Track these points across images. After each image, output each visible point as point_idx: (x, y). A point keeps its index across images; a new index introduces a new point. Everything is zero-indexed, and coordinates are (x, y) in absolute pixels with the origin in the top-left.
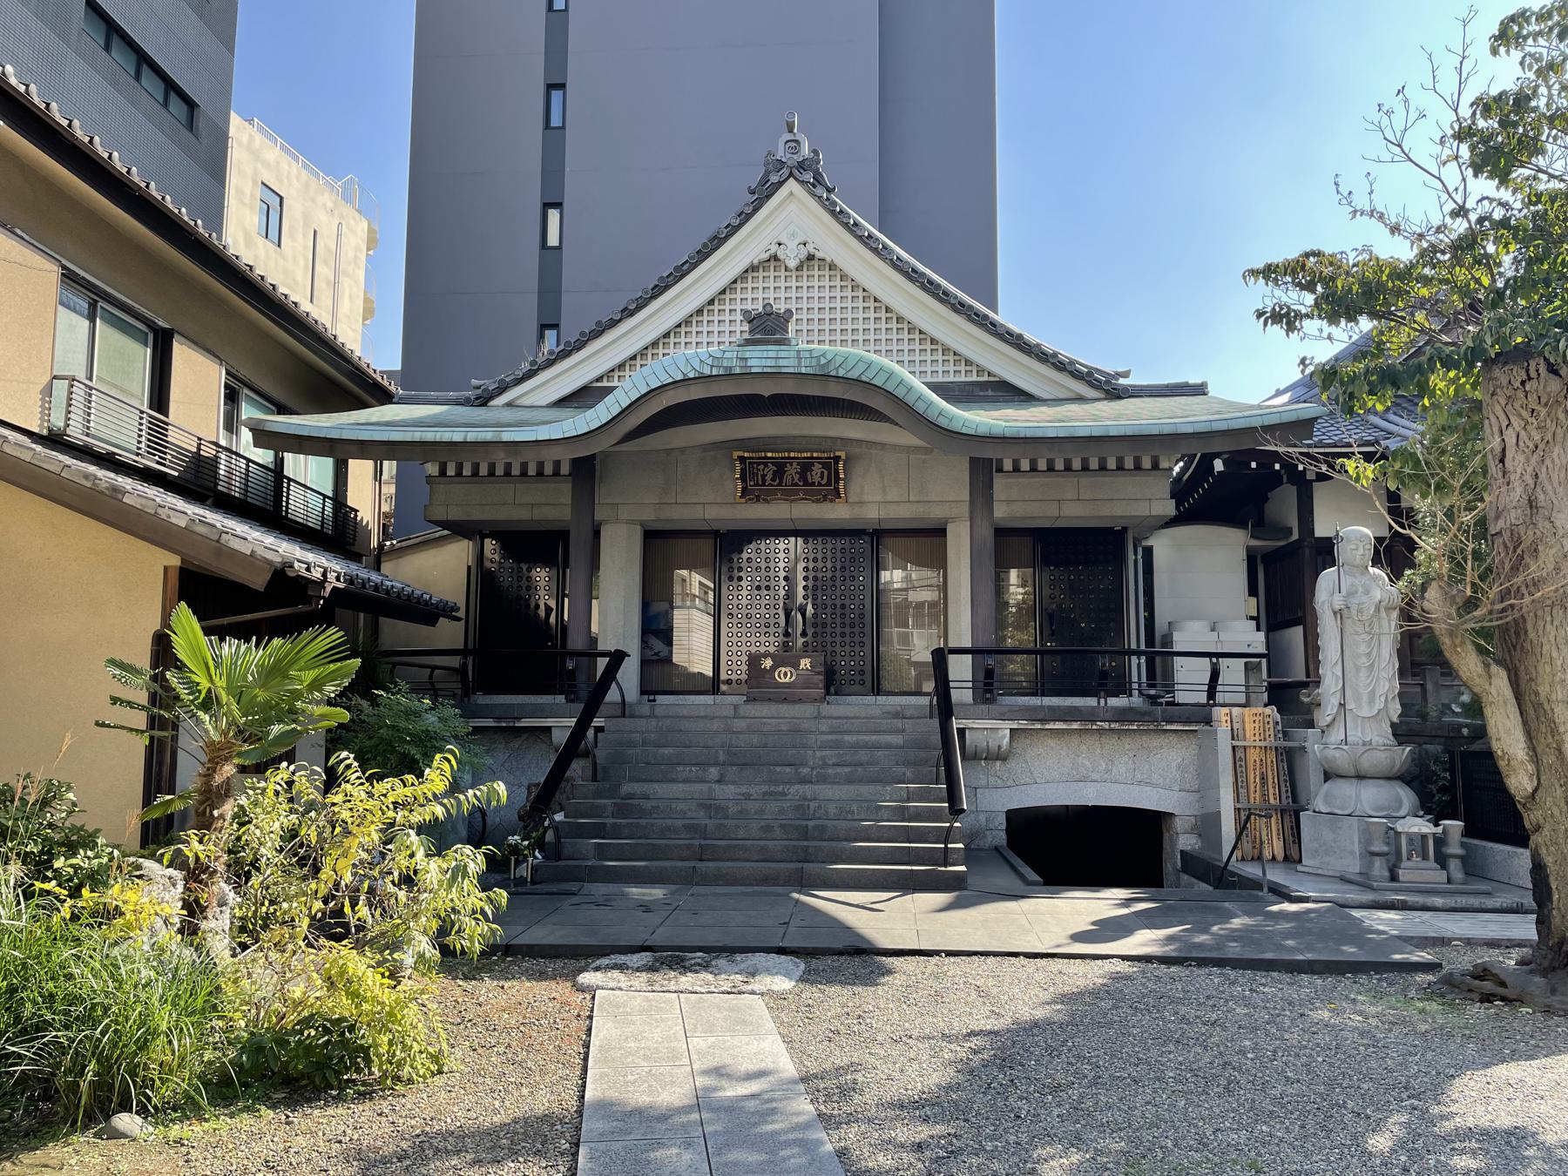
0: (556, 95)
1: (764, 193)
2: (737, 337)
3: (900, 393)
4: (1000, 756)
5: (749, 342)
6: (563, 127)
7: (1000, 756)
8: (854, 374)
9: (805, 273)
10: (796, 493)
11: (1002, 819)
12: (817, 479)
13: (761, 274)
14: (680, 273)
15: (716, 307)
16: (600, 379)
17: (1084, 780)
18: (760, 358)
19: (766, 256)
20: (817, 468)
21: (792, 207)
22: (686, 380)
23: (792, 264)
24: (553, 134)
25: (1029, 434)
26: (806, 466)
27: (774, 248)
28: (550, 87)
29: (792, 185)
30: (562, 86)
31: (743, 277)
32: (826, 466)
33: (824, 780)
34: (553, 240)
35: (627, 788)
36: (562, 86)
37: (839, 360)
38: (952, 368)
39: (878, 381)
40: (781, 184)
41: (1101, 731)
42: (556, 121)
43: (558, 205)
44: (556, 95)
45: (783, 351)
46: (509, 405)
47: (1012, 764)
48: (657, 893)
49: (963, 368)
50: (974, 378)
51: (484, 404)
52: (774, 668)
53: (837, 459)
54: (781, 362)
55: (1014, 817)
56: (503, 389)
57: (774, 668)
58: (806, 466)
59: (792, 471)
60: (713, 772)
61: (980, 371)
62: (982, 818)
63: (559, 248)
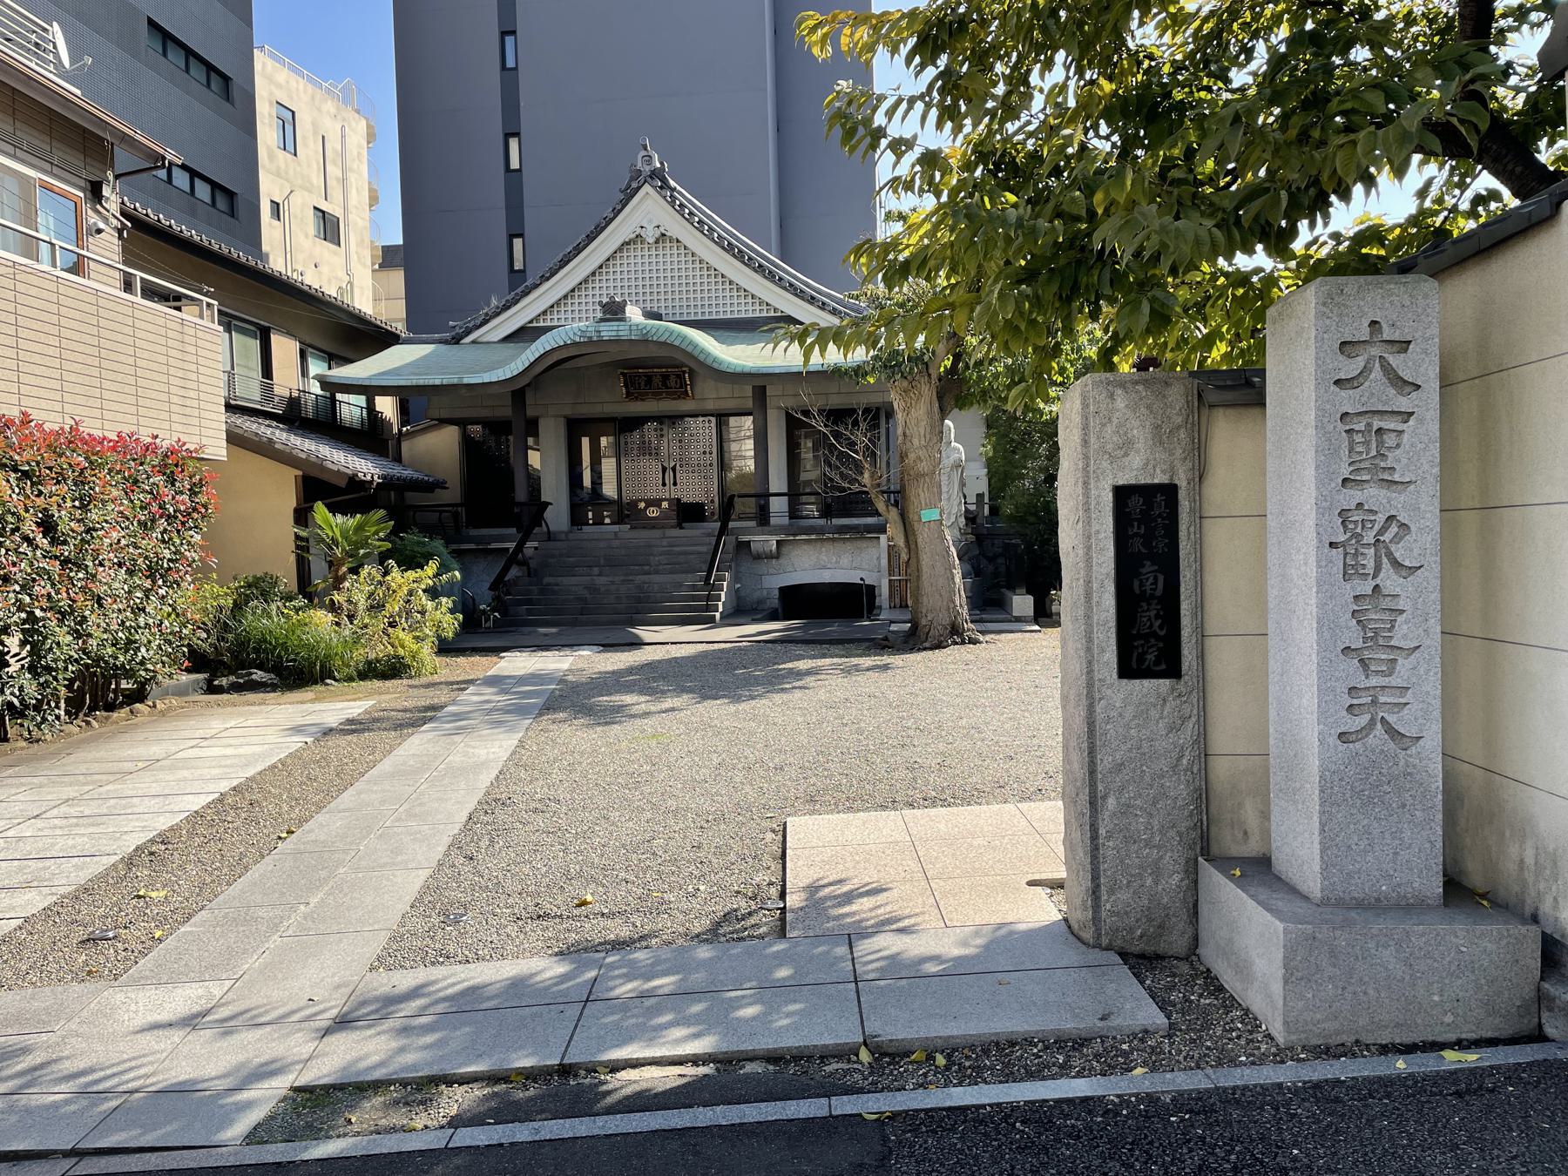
0: (509, 40)
1: (629, 194)
2: (599, 315)
3: (689, 349)
4: (771, 556)
5: (602, 320)
6: (516, 69)
7: (771, 556)
8: (662, 339)
9: (661, 245)
10: (661, 393)
11: (777, 592)
12: (673, 384)
13: (632, 246)
14: (578, 250)
15: (604, 270)
16: (531, 322)
17: (825, 568)
18: (609, 331)
19: (634, 236)
20: (673, 378)
21: (649, 202)
22: (566, 345)
23: (651, 241)
24: (509, 75)
25: (765, 371)
26: (665, 377)
27: (639, 231)
28: (504, 34)
29: (647, 188)
30: (513, 33)
31: (620, 249)
32: (678, 376)
33: (657, 572)
34: (515, 164)
35: (547, 580)
36: (513, 33)
37: (654, 331)
38: (758, 308)
39: (676, 343)
40: (639, 188)
41: (833, 540)
42: (510, 63)
43: (517, 135)
44: (509, 40)
45: (622, 326)
46: (474, 342)
47: (782, 561)
48: (554, 630)
49: (765, 307)
50: (772, 314)
51: (457, 343)
52: (646, 508)
53: (684, 372)
54: (621, 333)
55: (782, 589)
56: (468, 332)
57: (646, 508)
58: (665, 377)
59: (657, 380)
60: (596, 570)
61: (775, 310)
62: (765, 592)
63: (519, 170)
